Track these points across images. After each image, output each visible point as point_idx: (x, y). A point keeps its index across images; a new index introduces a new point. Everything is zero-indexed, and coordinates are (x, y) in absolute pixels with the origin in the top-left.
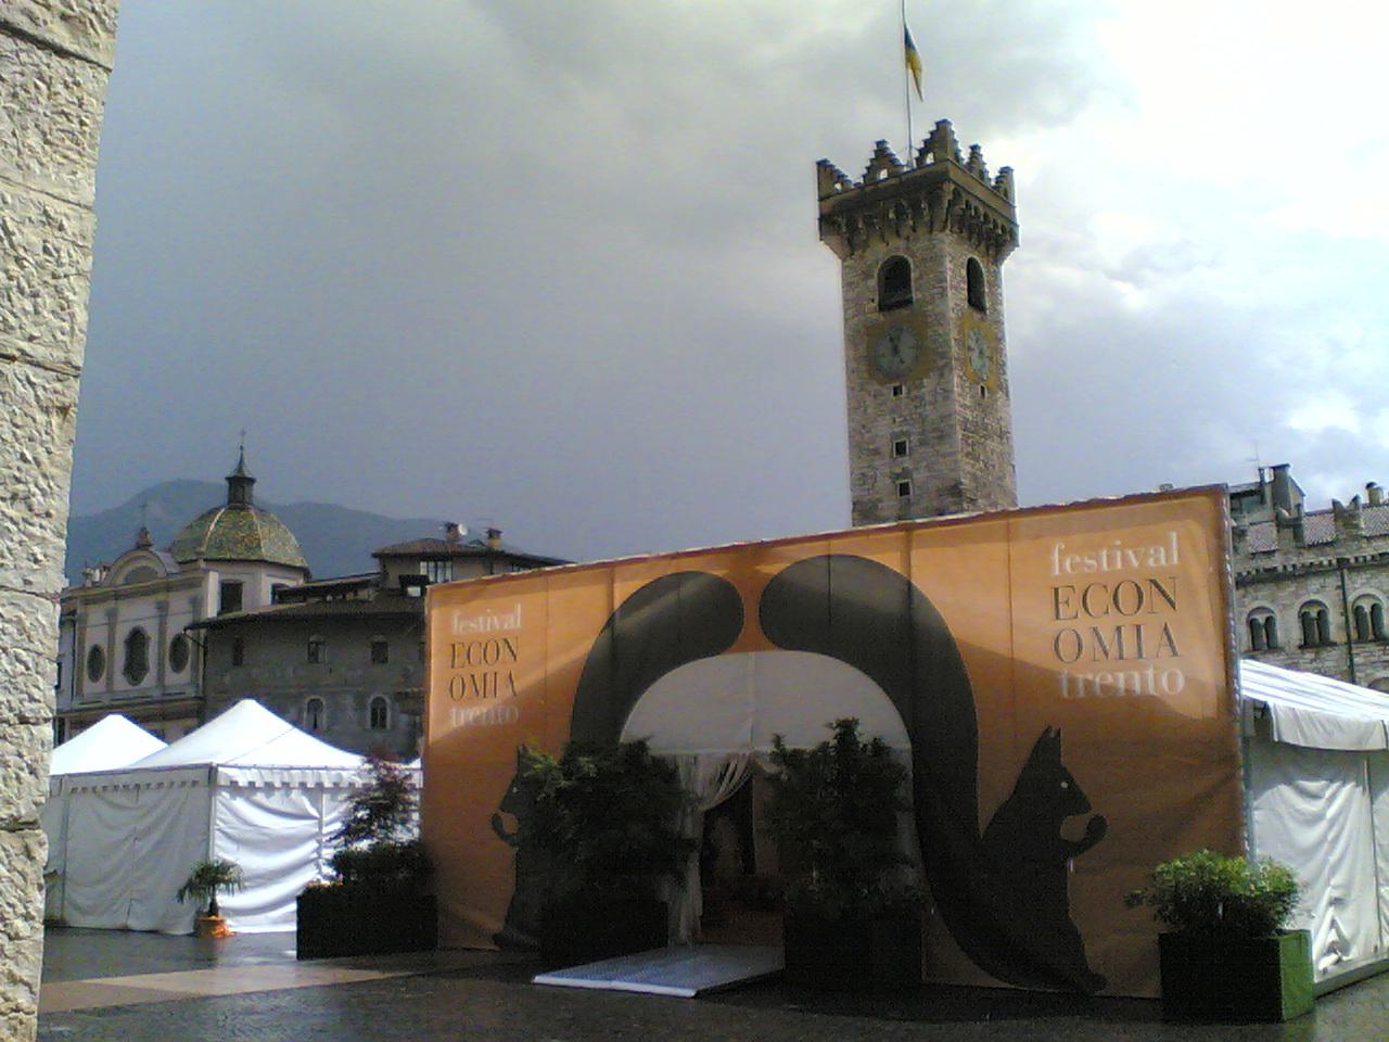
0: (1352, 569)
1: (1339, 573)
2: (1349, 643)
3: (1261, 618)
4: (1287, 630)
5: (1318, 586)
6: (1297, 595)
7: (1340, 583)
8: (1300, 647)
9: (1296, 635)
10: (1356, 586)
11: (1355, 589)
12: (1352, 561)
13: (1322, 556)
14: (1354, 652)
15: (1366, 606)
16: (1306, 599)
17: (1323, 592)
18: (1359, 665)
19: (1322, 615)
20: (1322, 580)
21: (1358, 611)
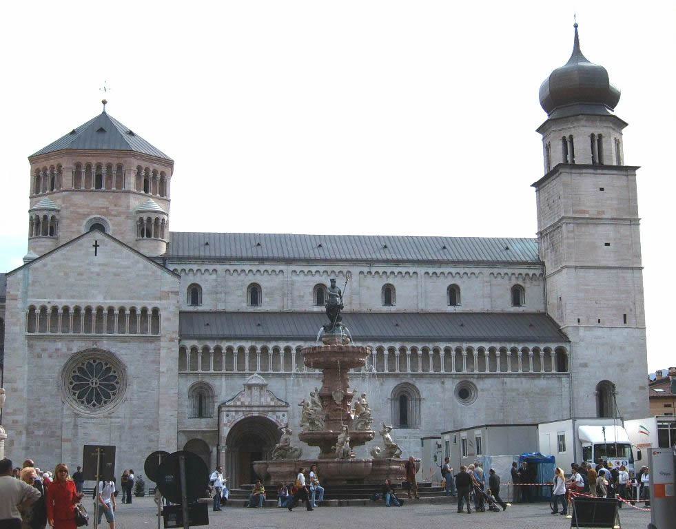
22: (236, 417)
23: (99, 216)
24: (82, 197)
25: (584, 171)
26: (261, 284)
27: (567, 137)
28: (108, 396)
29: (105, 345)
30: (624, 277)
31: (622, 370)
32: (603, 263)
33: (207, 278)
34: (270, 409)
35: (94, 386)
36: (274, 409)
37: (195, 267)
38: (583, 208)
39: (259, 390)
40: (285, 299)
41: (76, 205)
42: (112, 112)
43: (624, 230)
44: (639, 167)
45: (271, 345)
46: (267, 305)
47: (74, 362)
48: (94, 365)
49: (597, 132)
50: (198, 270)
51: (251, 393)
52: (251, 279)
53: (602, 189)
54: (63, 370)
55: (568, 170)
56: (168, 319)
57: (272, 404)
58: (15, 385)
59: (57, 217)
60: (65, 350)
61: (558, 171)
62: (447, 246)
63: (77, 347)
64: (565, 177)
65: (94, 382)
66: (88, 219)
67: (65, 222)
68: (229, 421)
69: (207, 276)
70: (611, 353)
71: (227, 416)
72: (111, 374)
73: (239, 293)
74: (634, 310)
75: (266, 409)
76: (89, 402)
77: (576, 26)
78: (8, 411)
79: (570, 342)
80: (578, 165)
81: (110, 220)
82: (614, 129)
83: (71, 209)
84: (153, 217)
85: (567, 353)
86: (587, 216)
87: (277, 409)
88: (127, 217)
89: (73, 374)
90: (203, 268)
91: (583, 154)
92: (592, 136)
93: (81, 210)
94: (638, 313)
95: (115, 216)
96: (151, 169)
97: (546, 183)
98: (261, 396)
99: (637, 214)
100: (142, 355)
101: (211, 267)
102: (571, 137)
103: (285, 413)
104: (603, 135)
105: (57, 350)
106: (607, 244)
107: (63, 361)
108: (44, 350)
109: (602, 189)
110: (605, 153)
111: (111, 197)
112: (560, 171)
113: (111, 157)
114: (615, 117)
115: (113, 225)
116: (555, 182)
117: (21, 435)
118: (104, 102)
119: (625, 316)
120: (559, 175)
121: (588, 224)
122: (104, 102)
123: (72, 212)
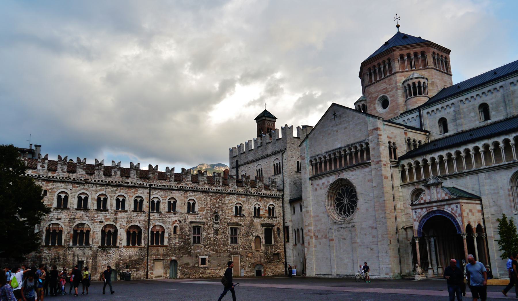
0: (153, 188)
1: (149, 189)
2: (149, 212)
3: (121, 199)
4: (130, 205)
5: (142, 192)
6: (135, 194)
7: (149, 192)
8: (133, 211)
9: (132, 206)
10: (153, 194)
11: (153, 195)
12: (153, 186)
13: (144, 182)
14: (150, 215)
15: (156, 200)
16: (137, 195)
17: (143, 194)
18: (151, 219)
19: (141, 201)
20: (143, 190)
21: (153, 202)
22: (422, 213)
23: (382, 95)
24: (373, 87)
26: (489, 103)
28: (353, 209)
29: (346, 175)
33: (449, 111)
34: (445, 203)
35: (346, 203)
36: (448, 201)
37: (439, 106)
39: (435, 188)
40: (508, 108)
41: (371, 93)
42: (402, 30)
45: (462, 149)
46: (495, 117)
47: (333, 191)
48: (345, 189)
50: (442, 107)
51: (430, 191)
52: (480, 101)
54: (328, 195)
56: (374, 149)
57: (447, 198)
58: (308, 209)
59: (365, 104)
60: (326, 183)
63: (332, 179)
65: (346, 201)
66: (378, 99)
67: (368, 105)
68: (417, 217)
69: (448, 110)
71: (416, 212)
72: (353, 194)
73: (473, 114)
75: (443, 203)
76: (345, 213)
78: (307, 224)
81: (388, 95)
83: (369, 97)
84: (410, 82)
87: (451, 202)
88: (397, 89)
89: (336, 197)
90: (444, 105)
93: (374, 95)
95: (391, 91)
96: (412, 53)
98: (437, 193)
100: (363, 177)
101: (449, 103)
103: (458, 205)
105: (323, 184)
107: (327, 189)
108: (318, 185)
111: (387, 81)
113: (383, 56)
115: (390, 97)
117: (312, 238)
118: (398, 26)
122: (398, 26)
123: (370, 98)
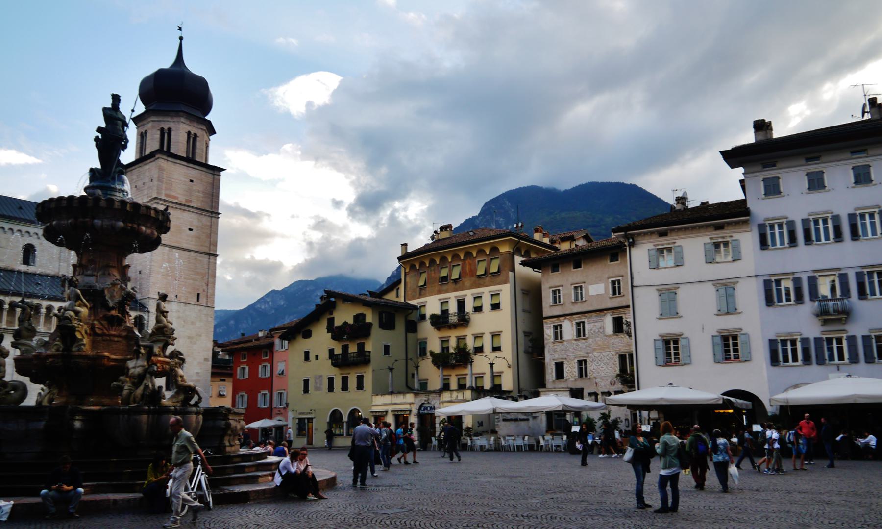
25: (178, 161)
27: (166, 128)
30: (201, 261)
31: (191, 342)
32: (185, 246)
38: (174, 194)
43: (206, 220)
44: (224, 170)
49: (193, 131)
53: (192, 181)
55: (165, 157)
61: (154, 156)
62: (23, 208)
64: (162, 162)
70: (184, 326)
74: (206, 290)
77: (181, 38)
79: (148, 312)
80: (172, 154)
82: (206, 133)
85: (145, 322)
86: (176, 201)
91: (179, 145)
92: (189, 133)
94: (209, 294)
97: (137, 166)
99: (217, 208)
102: (170, 130)
104: (198, 135)
106: (191, 230)
109: (192, 181)
110: (198, 151)
112: (157, 156)
114: (210, 122)
116: (147, 167)
119: (198, 295)
120: (156, 159)
121: (176, 208)
